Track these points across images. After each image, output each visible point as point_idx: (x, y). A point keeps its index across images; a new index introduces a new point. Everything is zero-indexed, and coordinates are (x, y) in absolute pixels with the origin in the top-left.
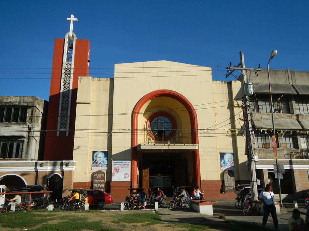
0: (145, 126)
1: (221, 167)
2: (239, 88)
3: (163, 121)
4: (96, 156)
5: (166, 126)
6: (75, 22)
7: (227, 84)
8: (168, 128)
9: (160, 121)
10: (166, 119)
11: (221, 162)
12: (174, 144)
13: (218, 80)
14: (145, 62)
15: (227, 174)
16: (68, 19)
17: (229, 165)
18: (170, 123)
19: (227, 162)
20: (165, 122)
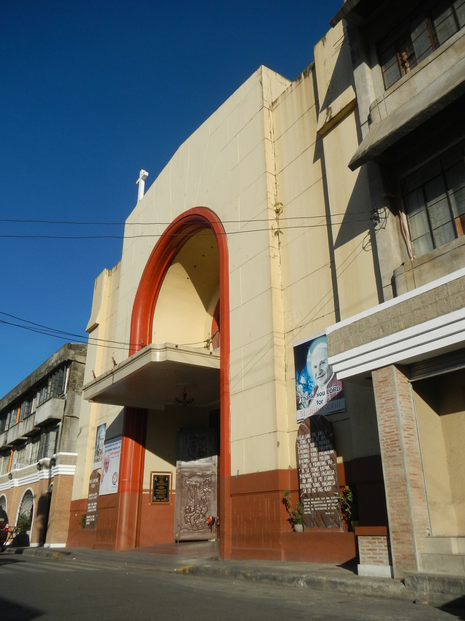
1: (299, 406)
2: (336, 52)
4: (99, 437)
11: (296, 390)
15: (308, 436)
17: (323, 394)
19: (318, 382)
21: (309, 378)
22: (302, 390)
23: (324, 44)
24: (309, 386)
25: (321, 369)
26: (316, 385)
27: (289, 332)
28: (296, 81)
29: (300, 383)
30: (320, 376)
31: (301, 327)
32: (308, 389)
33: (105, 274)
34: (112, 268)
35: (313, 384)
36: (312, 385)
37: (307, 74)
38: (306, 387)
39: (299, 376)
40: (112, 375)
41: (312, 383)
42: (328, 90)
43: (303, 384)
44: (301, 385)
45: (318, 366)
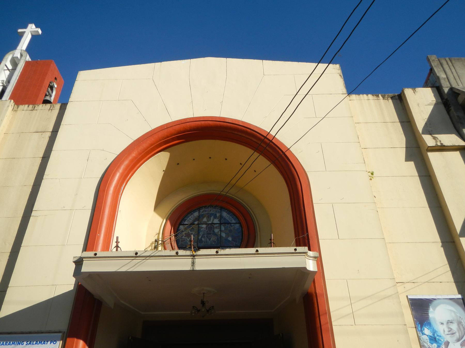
0: (159, 234)
2: (429, 105)
3: (216, 221)
5: (224, 235)
6: (34, 37)
7: (390, 101)
8: (230, 239)
9: (205, 220)
10: (225, 214)
11: (419, 339)
12: (213, 251)
13: (363, 94)
14: (157, 65)
16: (20, 30)
18: (237, 226)
20: (221, 224)
21: (436, 332)
22: (428, 340)
23: (414, 92)
24: (437, 339)
25: (450, 327)
26: (445, 340)
27: (399, 283)
28: (373, 95)
29: (423, 334)
30: (449, 333)
31: (414, 282)
32: (436, 341)
33: (10, 106)
34: (22, 104)
35: (442, 339)
36: (440, 339)
37: (386, 98)
38: (433, 339)
39: (421, 327)
40: (192, 257)
41: (441, 337)
42: (426, 124)
43: (429, 336)
44: (426, 336)
45: (445, 323)
